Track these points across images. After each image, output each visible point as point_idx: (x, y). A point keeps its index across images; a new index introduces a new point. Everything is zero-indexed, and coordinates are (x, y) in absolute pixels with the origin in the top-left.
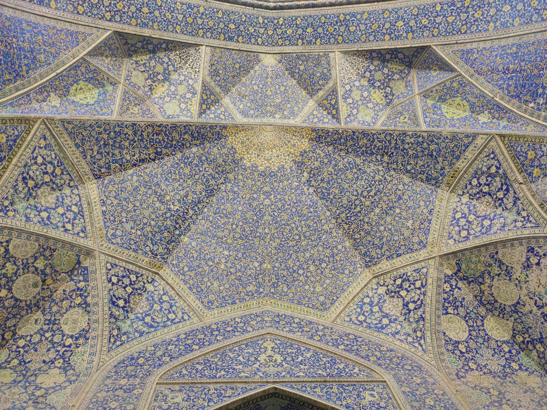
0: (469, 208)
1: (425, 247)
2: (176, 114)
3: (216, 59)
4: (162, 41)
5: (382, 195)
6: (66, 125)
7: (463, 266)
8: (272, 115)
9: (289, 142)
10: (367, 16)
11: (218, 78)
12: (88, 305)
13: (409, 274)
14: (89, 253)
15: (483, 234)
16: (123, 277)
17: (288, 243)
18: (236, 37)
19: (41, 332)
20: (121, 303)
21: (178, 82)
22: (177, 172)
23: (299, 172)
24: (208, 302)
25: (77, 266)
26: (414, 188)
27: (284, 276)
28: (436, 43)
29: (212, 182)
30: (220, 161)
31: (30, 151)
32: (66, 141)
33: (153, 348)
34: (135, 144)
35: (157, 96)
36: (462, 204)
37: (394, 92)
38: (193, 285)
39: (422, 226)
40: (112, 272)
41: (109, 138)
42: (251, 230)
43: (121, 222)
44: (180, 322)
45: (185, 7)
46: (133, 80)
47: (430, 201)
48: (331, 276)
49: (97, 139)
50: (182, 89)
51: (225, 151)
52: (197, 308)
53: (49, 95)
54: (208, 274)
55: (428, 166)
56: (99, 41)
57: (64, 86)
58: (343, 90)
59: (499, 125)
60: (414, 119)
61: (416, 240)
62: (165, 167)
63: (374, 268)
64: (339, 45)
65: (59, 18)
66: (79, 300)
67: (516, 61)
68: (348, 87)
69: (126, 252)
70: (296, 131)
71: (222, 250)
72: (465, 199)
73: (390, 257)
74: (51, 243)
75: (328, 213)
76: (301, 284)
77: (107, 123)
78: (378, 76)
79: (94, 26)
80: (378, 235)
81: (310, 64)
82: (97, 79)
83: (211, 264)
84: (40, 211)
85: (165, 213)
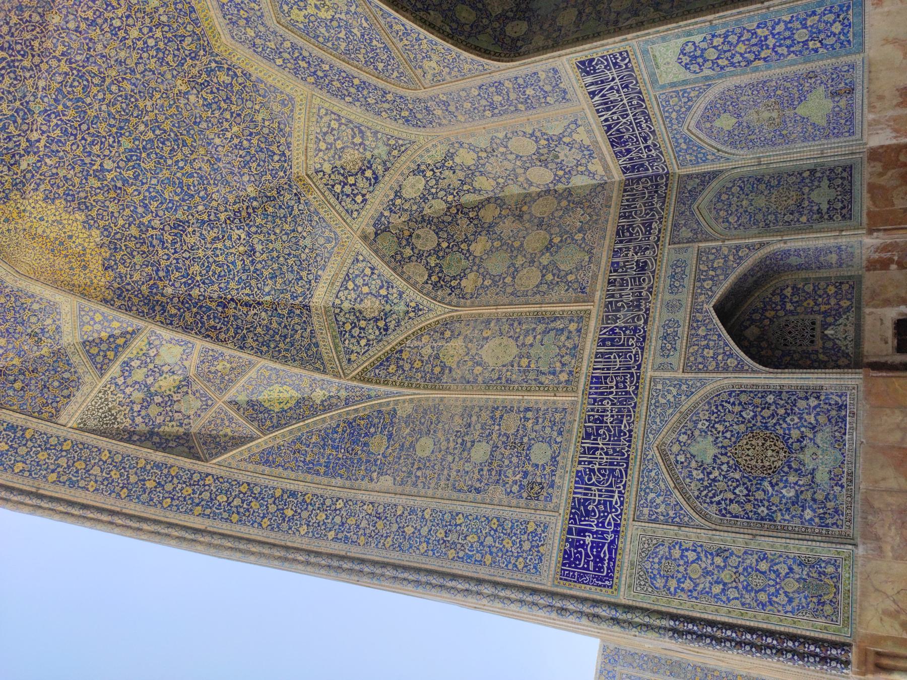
3: (55, 405)
4: (138, 443)
9: (9, 230)
12: (396, 192)
14: (365, 238)
16: (348, 196)
19: (435, 196)
20: (369, 173)
22: (211, 273)
23: (29, 176)
24: (286, 106)
27: (175, 56)
29: (168, 237)
30: (138, 259)
31: (370, 352)
33: (384, 113)
34: (249, 326)
38: (284, 136)
40: (356, 207)
42: (163, 143)
43: (312, 250)
44: (332, 113)
49: (292, 345)
52: (303, 111)
53: (322, 401)
54: (258, 134)
56: (234, 452)
57: (300, 408)
62: (222, 285)
66: (398, 202)
69: (327, 217)
71: (220, 148)
74: (393, 264)
75: (42, 83)
76: (166, 29)
77: (273, 358)
82: (255, 411)
83: (245, 142)
85: (256, 233)
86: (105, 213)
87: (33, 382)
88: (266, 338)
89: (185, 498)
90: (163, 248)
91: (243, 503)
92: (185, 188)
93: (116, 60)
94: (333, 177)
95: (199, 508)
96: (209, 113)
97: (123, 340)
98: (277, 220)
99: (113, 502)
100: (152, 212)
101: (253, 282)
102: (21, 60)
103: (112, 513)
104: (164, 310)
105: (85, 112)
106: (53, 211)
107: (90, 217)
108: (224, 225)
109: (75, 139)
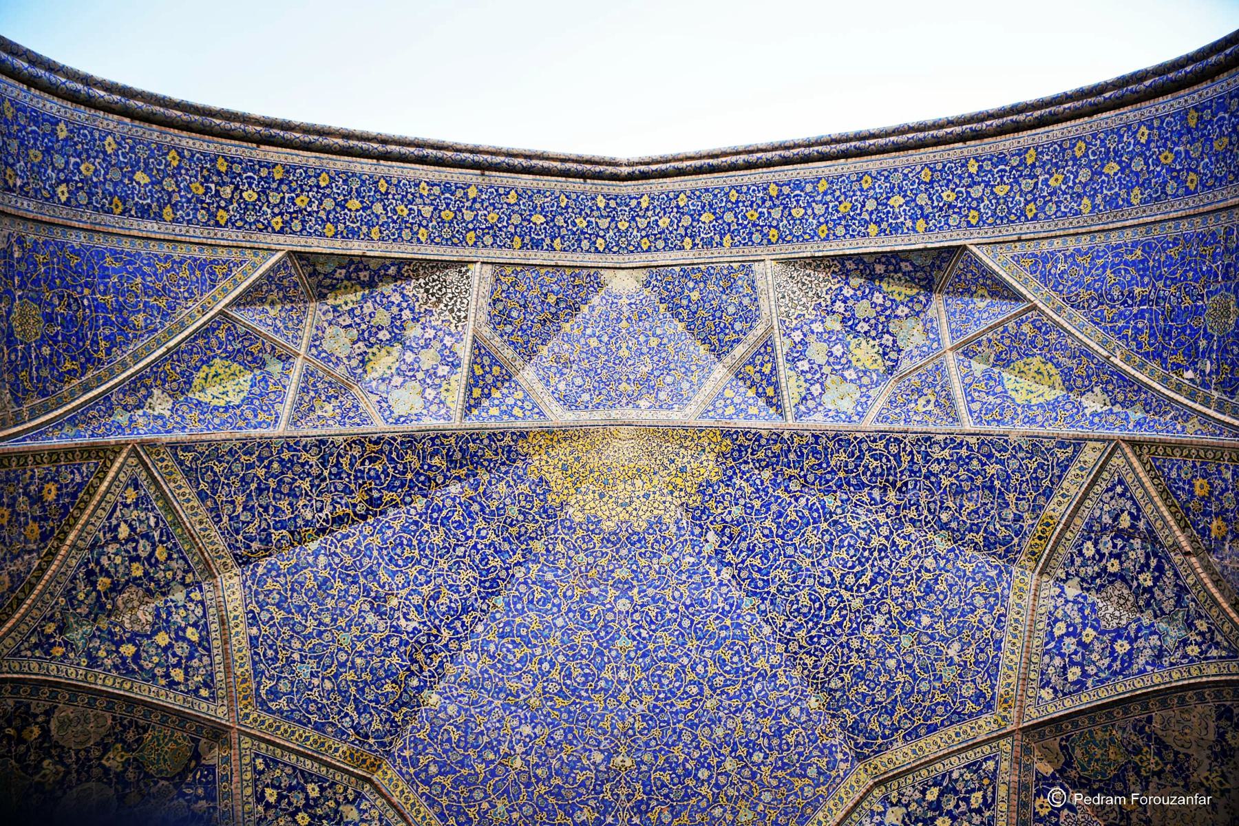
0: (1081, 610)
1: (989, 706)
2: (413, 412)
3: (505, 287)
4: (388, 262)
5: (889, 583)
6: (180, 453)
7: (1078, 753)
8: (632, 400)
10: (827, 186)
11: (509, 329)
13: (955, 775)
14: (218, 734)
15: (1115, 673)
16: (291, 788)
17: (672, 705)
18: (548, 241)
21: (422, 342)
22: (415, 542)
23: (697, 531)
25: (193, 763)
26: (959, 564)
27: (663, 785)
28: (976, 241)
29: (495, 562)
30: (513, 512)
32: (180, 487)
34: (323, 485)
35: (375, 375)
36: (1067, 602)
37: (900, 344)
38: (449, 807)
39: (982, 657)
41: (269, 474)
42: (586, 675)
43: (290, 662)
45: (436, 190)
46: (325, 346)
47: (996, 596)
48: (775, 783)
50: (428, 359)
51: (523, 488)
53: (150, 395)
55: (987, 513)
56: (257, 275)
57: (182, 373)
58: (788, 341)
59: (1127, 418)
60: (947, 405)
61: (968, 690)
62: (389, 532)
63: (877, 761)
64: (771, 247)
65: (179, 238)
67: (1146, 280)
68: (797, 336)
70: (686, 437)
71: (516, 723)
72: (1072, 591)
73: (913, 734)
74: (139, 712)
75: (767, 630)
76: (704, 804)
78: (863, 309)
79: (248, 245)
80: (882, 679)
81: (711, 287)
82: (250, 353)
83: (491, 756)
84: (119, 644)
85: (388, 638)
86: (584, 546)
87: (539, 308)
88: (290, 474)
89: (302, 191)
90: (492, 544)
91: (217, 191)
92: (518, 640)
93: (720, 721)
94: (332, 804)
95: (277, 177)
96: (565, 757)
97: (475, 395)
98: (369, 678)
99: (393, 172)
100: (534, 583)
101: (348, 560)
102: (809, 632)
103: (387, 157)
104: (449, 458)
105: (699, 639)
106: (641, 513)
107: (597, 531)
108: (437, 622)
109: (684, 604)
